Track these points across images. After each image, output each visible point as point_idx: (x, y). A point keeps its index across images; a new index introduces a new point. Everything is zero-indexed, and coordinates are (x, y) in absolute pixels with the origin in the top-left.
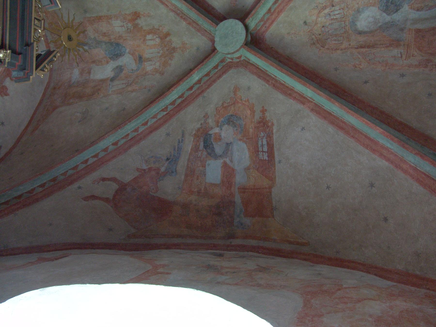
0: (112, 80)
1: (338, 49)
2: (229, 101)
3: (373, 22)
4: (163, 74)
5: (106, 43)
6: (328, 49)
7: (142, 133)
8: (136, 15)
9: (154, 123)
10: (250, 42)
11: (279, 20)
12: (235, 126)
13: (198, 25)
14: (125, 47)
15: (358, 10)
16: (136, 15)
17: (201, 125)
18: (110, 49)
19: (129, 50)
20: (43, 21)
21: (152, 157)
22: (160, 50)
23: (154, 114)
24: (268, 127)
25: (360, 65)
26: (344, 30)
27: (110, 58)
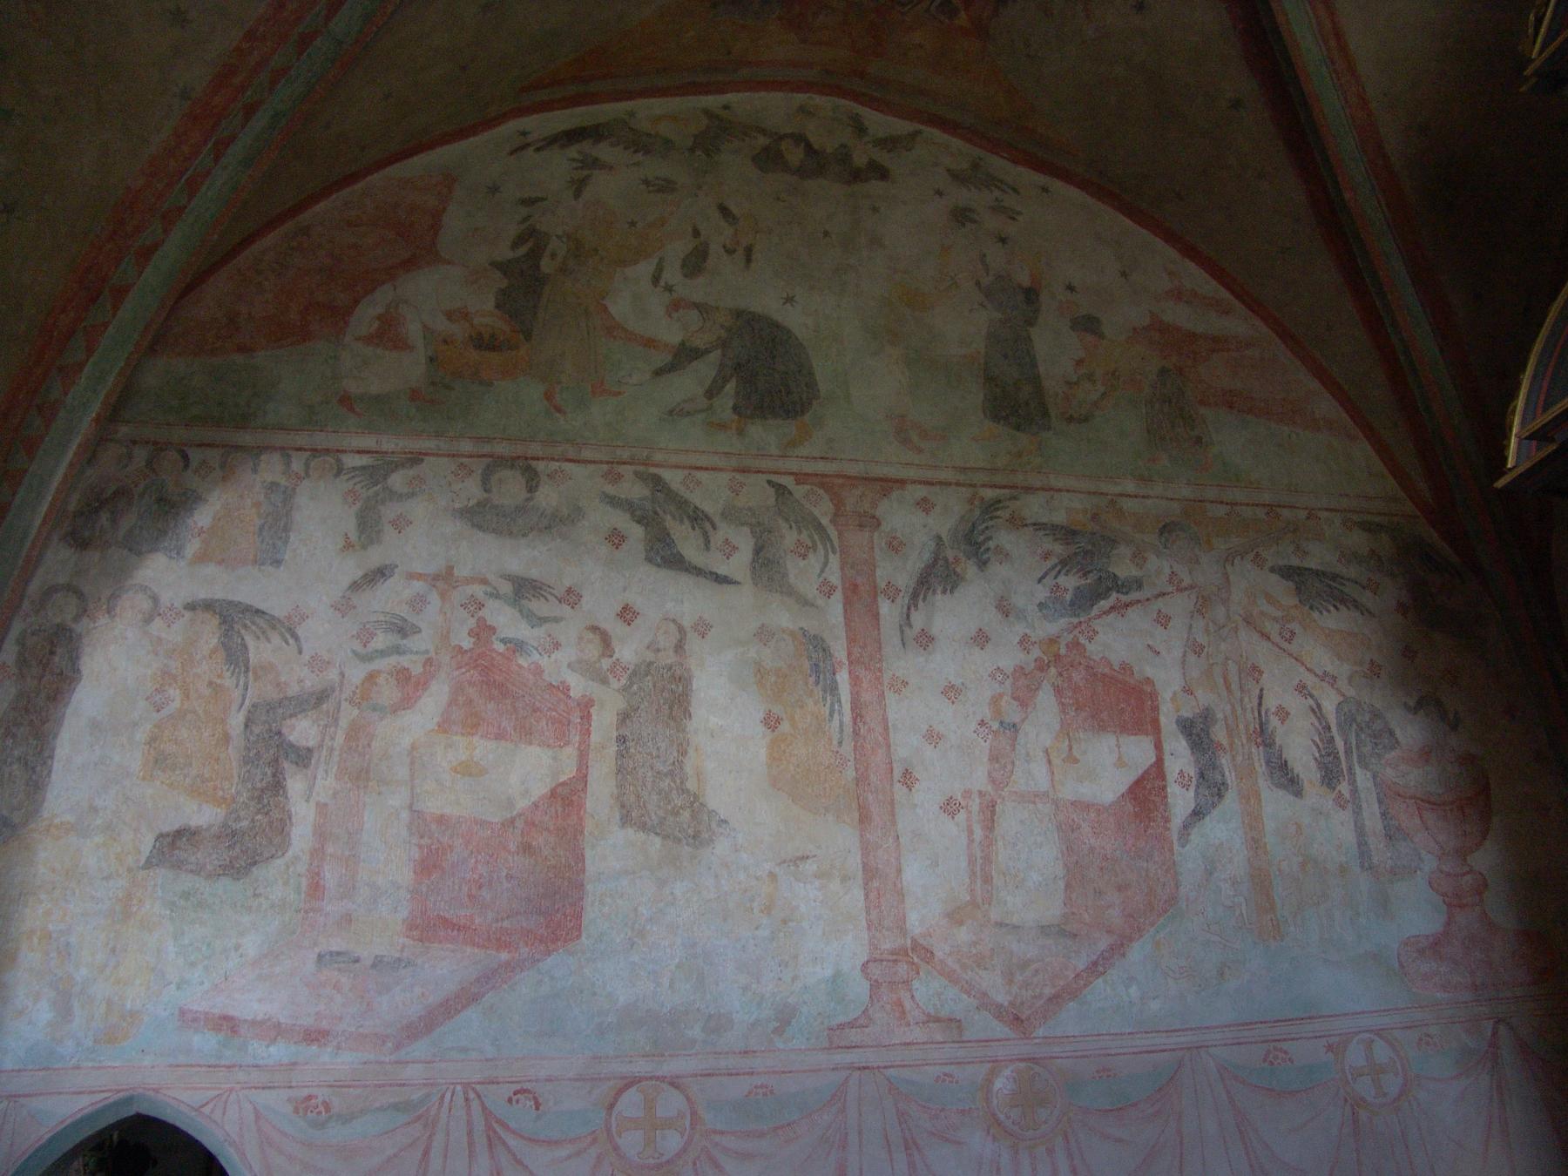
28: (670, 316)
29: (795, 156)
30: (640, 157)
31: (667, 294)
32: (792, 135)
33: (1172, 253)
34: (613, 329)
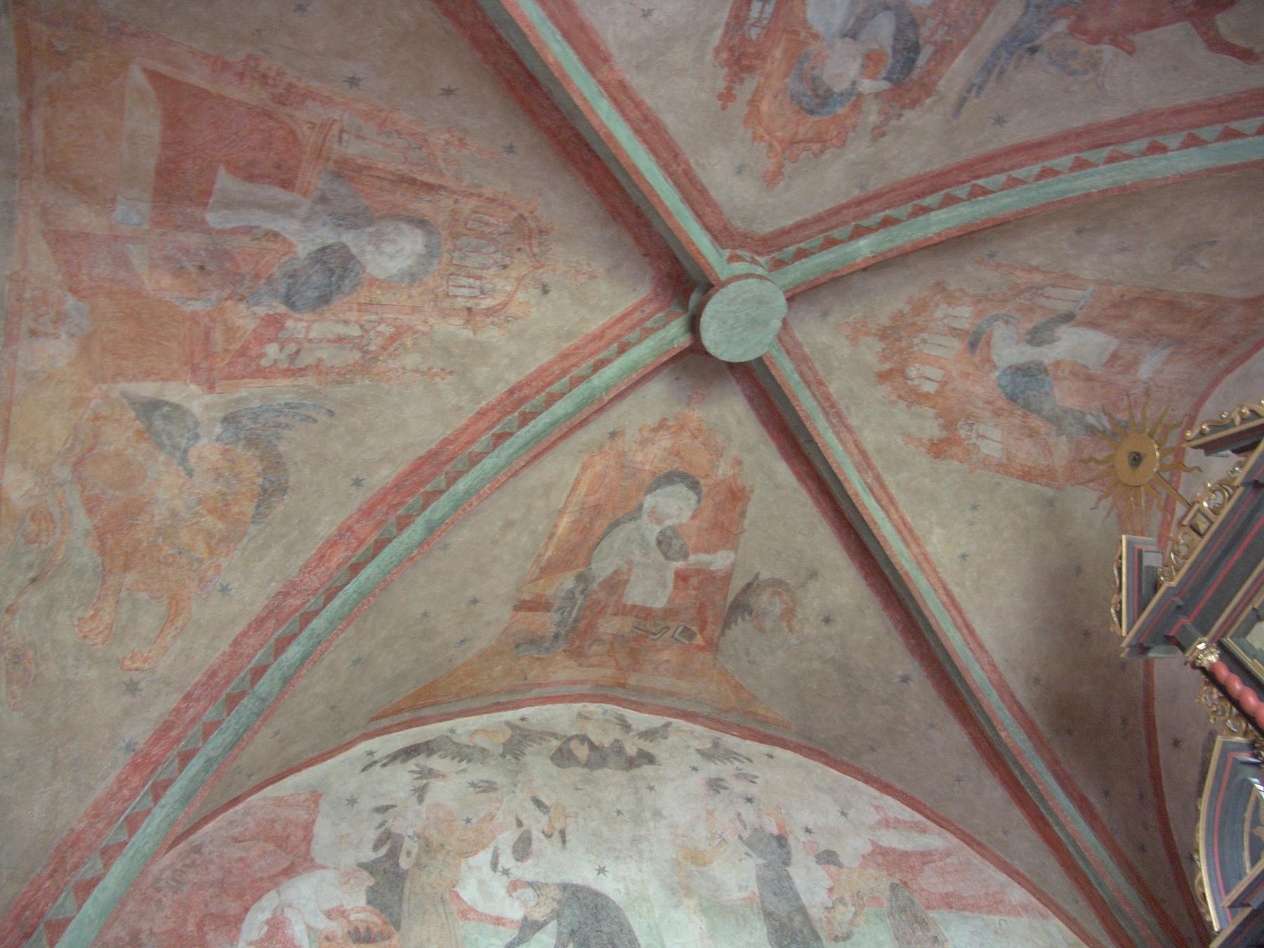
0: (1068, 318)
1: (487, 198)
2: (804, 154)
3: (383, 240)
4: (938, 284)
5: (1039, 412)
6: (512, 208)
7: (1068, 152)
8: (937, 449)
9: (1022, 166)
10: (697, 289)
11: (606, 319)
12: (814, 79)
13: (802, 375)
14: (999, 385)
15: (414, 281)
16: (937, 449)
17: (900, 116)
18: (1035, 393)
19: (992, 375)
20: (1185, 522)
21: (1072, 73)
22: (917, 345)
23: (1012, 191)
24: (731, 49)
25: (447, 143)
26: (458, 242)
27: (1046, 371)
28: (511, 896)
29: (582, 752)
30: (464, 765)
31: (505, 876)
32: (577, 736)
33: (873, 791)
34: (466, 912)
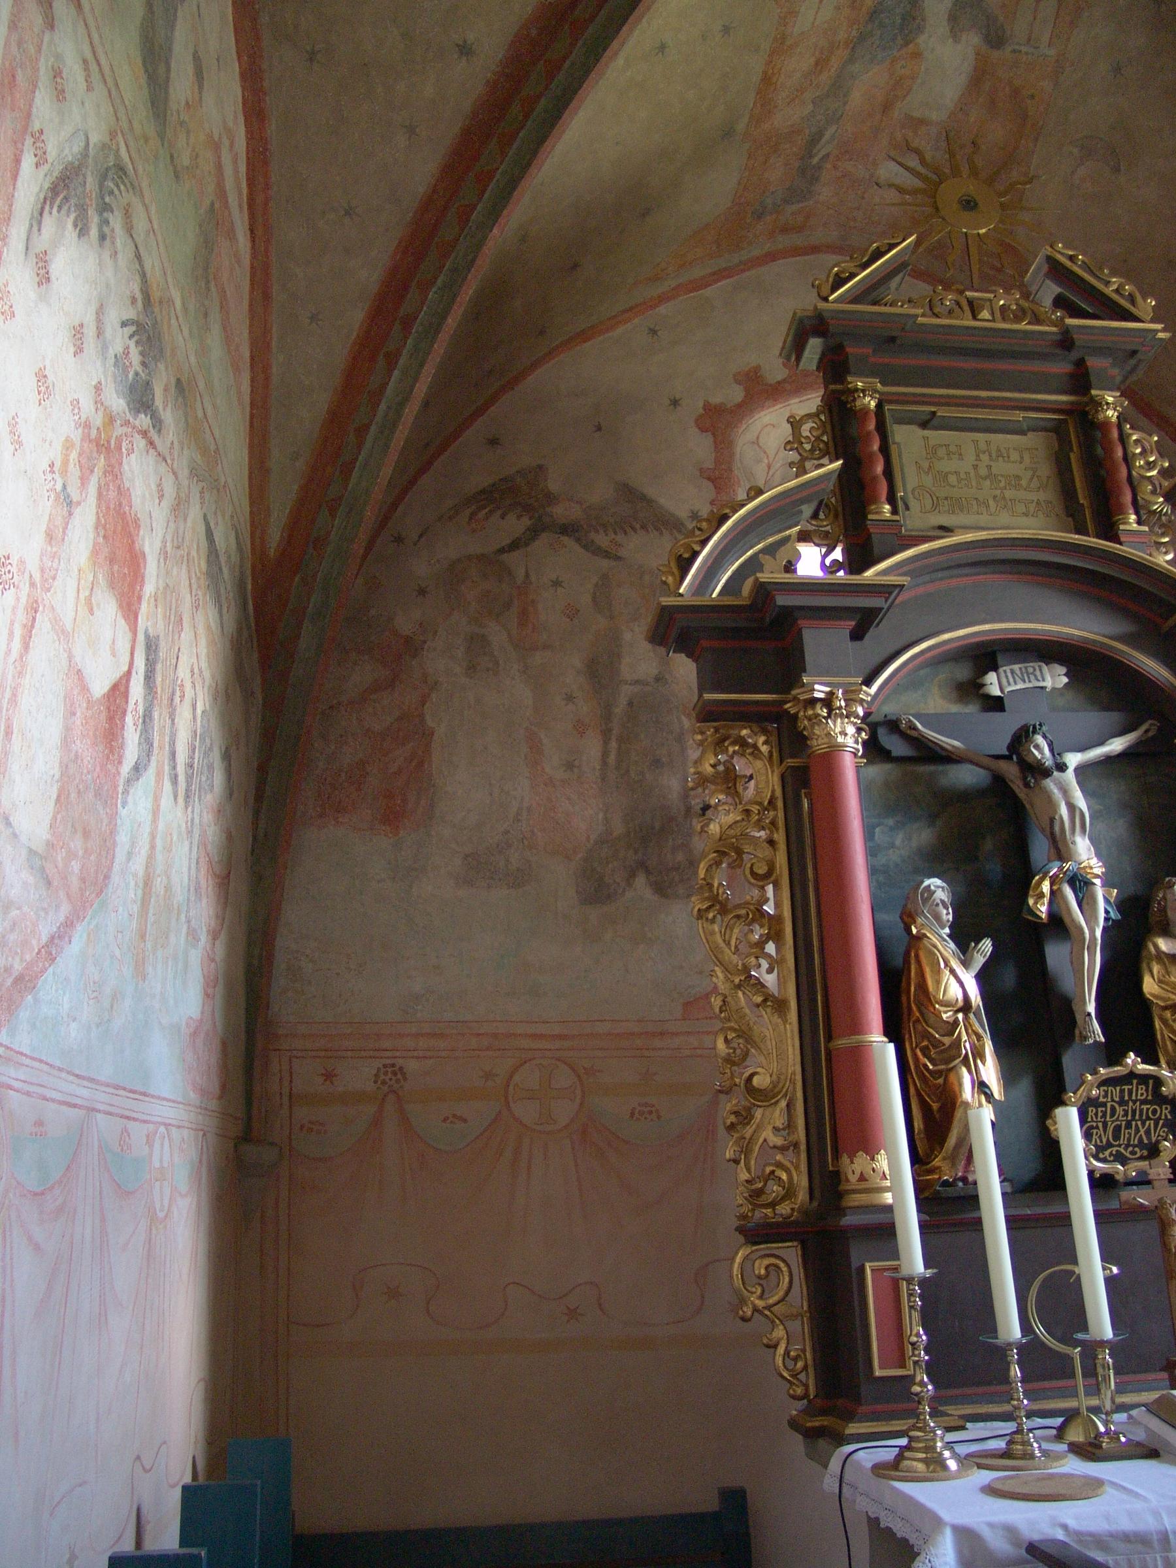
0: (995, 38)
5: (851, 60)
27: (907, 44)
